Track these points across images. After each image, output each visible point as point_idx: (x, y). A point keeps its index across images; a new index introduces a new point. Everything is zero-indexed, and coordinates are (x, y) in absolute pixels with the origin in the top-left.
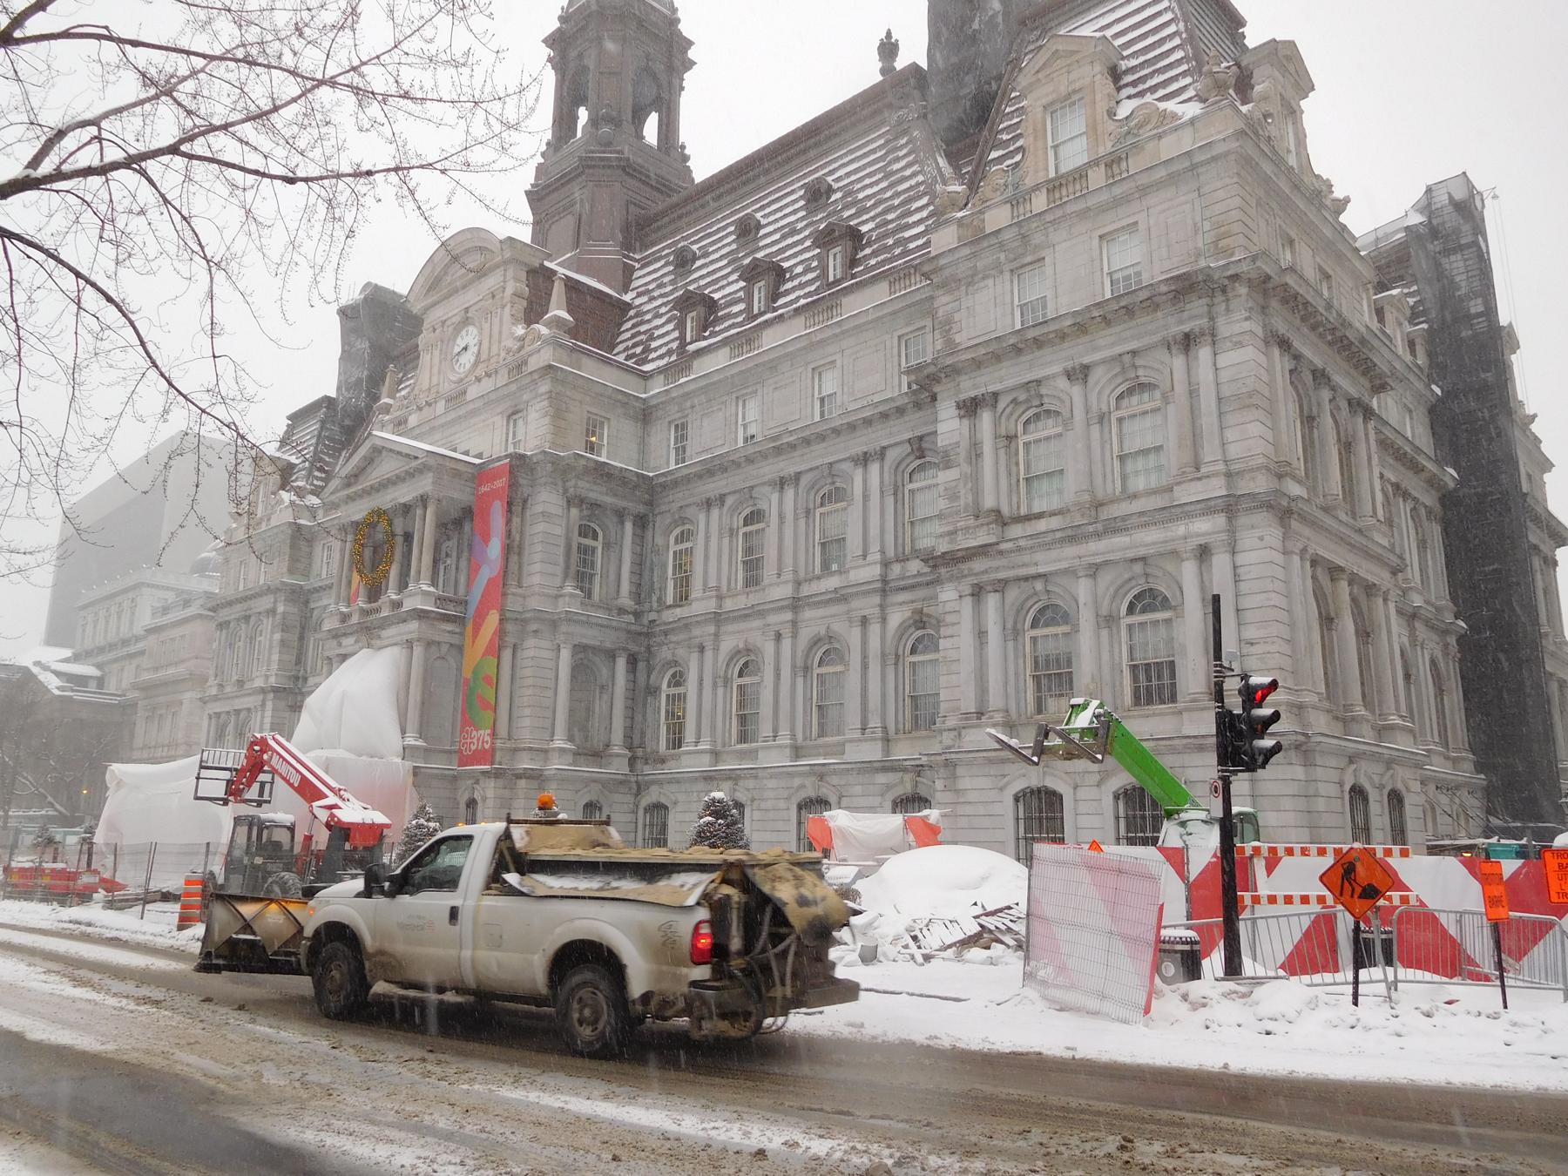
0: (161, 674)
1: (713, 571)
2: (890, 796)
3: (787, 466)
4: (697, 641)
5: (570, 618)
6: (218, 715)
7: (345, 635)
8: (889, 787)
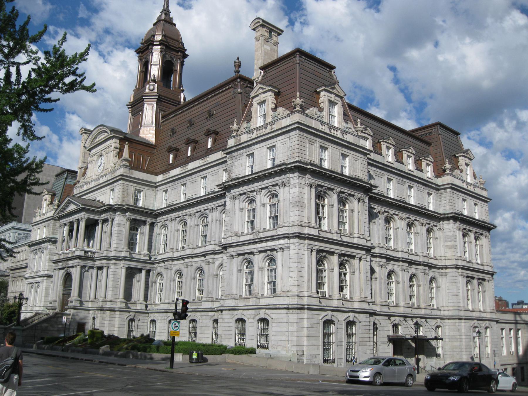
0: (18, 264)
1: (172, 243)
2: (212, 319)
3: (192, 210)
4: (166, 267)
5: (125, 259)
6: (31, 283)
7: (60, 262)
8: (212, 317)
